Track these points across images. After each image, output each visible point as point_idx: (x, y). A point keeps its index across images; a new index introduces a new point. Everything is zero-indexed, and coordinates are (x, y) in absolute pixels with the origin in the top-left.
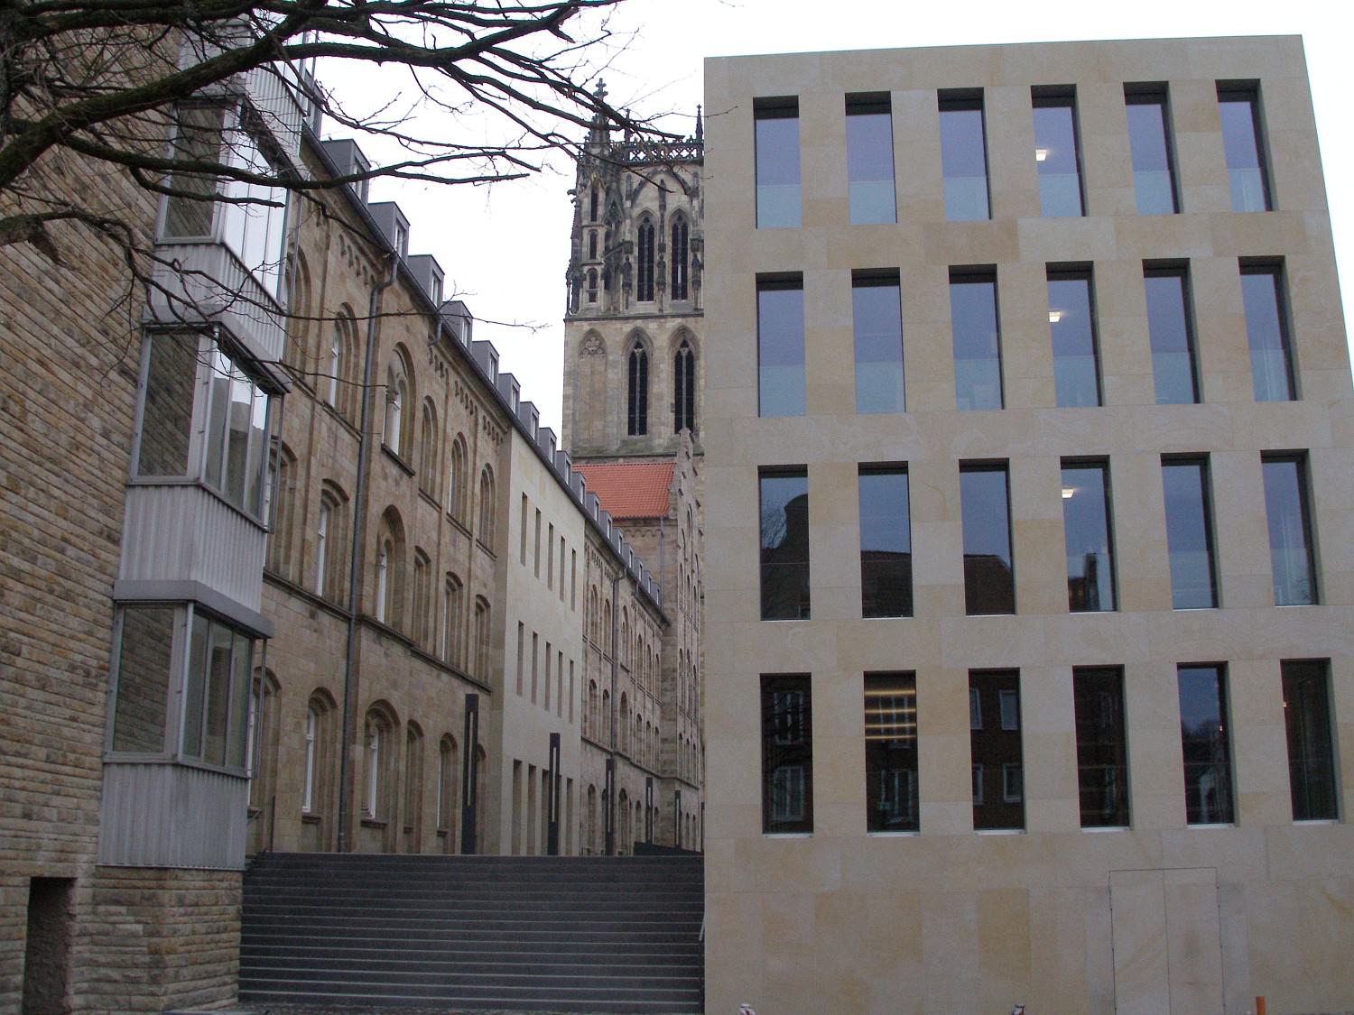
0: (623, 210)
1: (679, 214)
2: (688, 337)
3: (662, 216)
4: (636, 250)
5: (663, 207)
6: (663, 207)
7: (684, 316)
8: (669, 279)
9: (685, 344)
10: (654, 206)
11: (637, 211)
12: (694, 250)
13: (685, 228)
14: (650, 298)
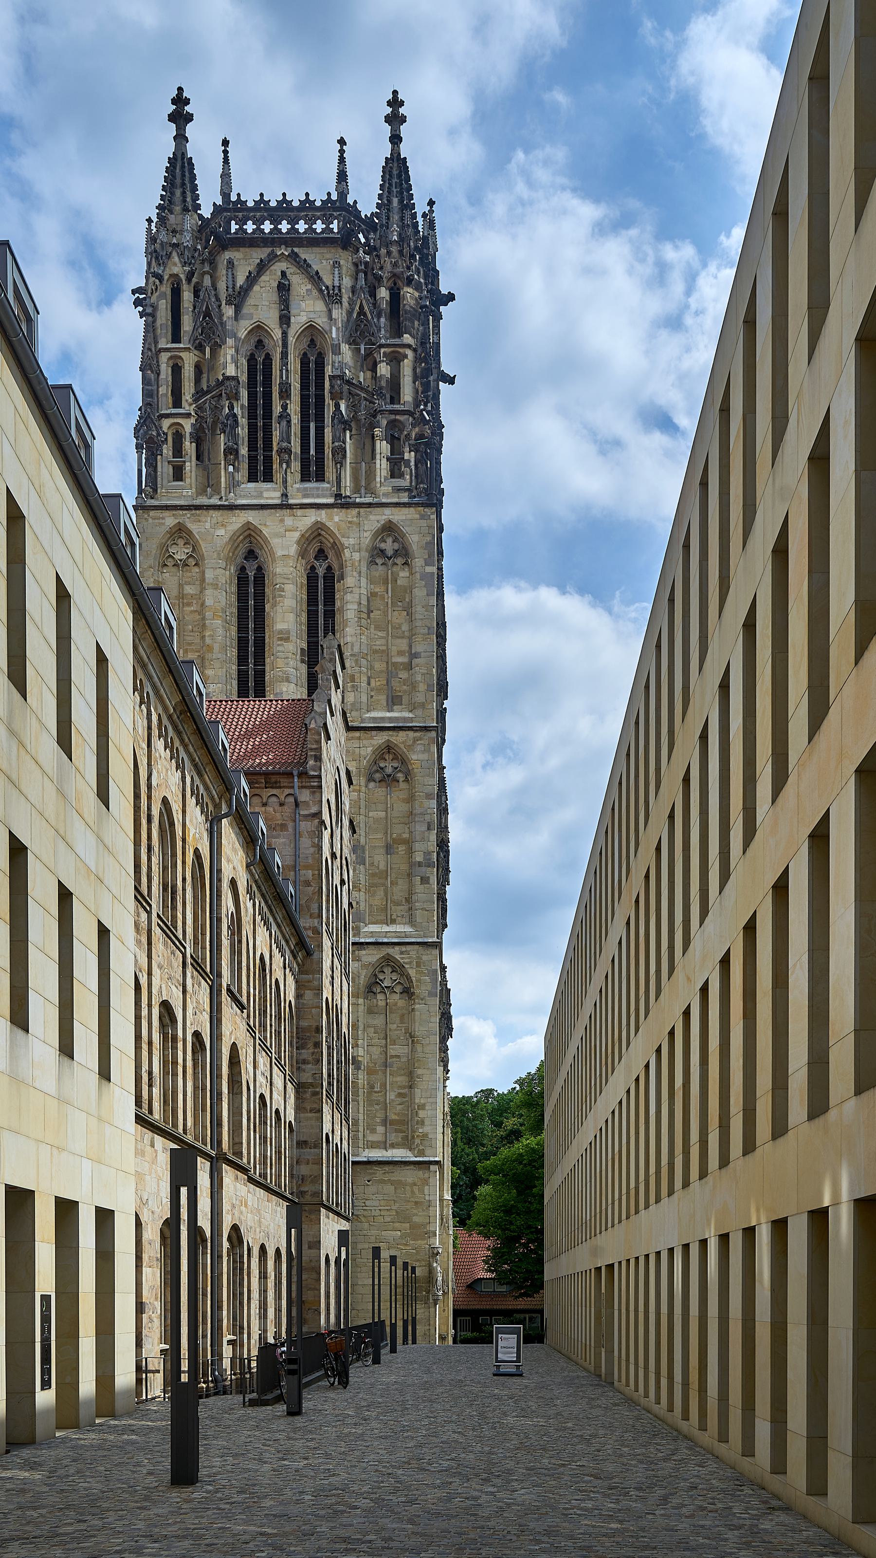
1: (312, 332)
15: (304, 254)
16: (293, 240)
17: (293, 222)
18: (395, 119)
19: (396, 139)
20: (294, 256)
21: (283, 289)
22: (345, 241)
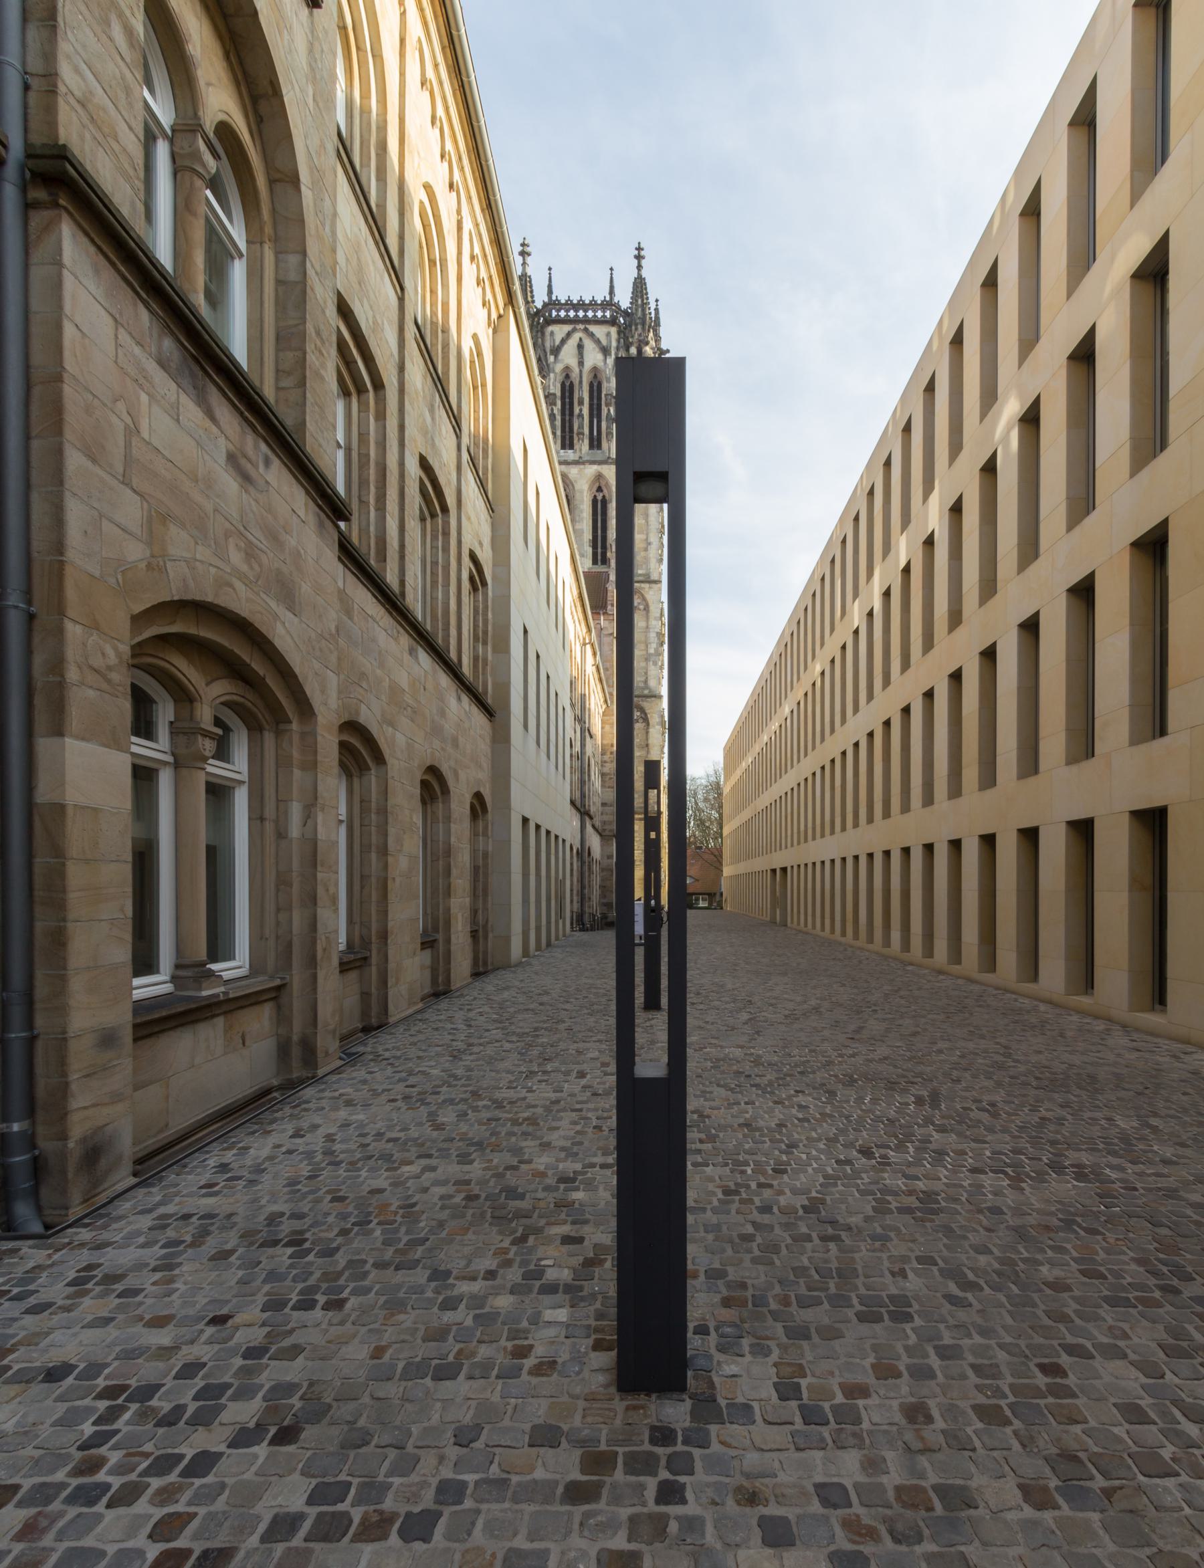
0: (548, 365)
1: (595, 372)
2: (603, 484)
3: (581, 371)
4: (559, 403)
5: (581, 363)
6: (581, 363)
7: (600, 463)
8: (586, 430)
9: (600, 489)
10: (573, 362)
11: (559, 367)
12: (607, 405)
13: (600, 384)
14: (571, 447)
15: (592, 328)
16: (586, 321)
17: (586, 311)
18: (639, 257)
19: (639, 267)
20: (586, 330)
21: (580, 347)
22: (613, 322)
